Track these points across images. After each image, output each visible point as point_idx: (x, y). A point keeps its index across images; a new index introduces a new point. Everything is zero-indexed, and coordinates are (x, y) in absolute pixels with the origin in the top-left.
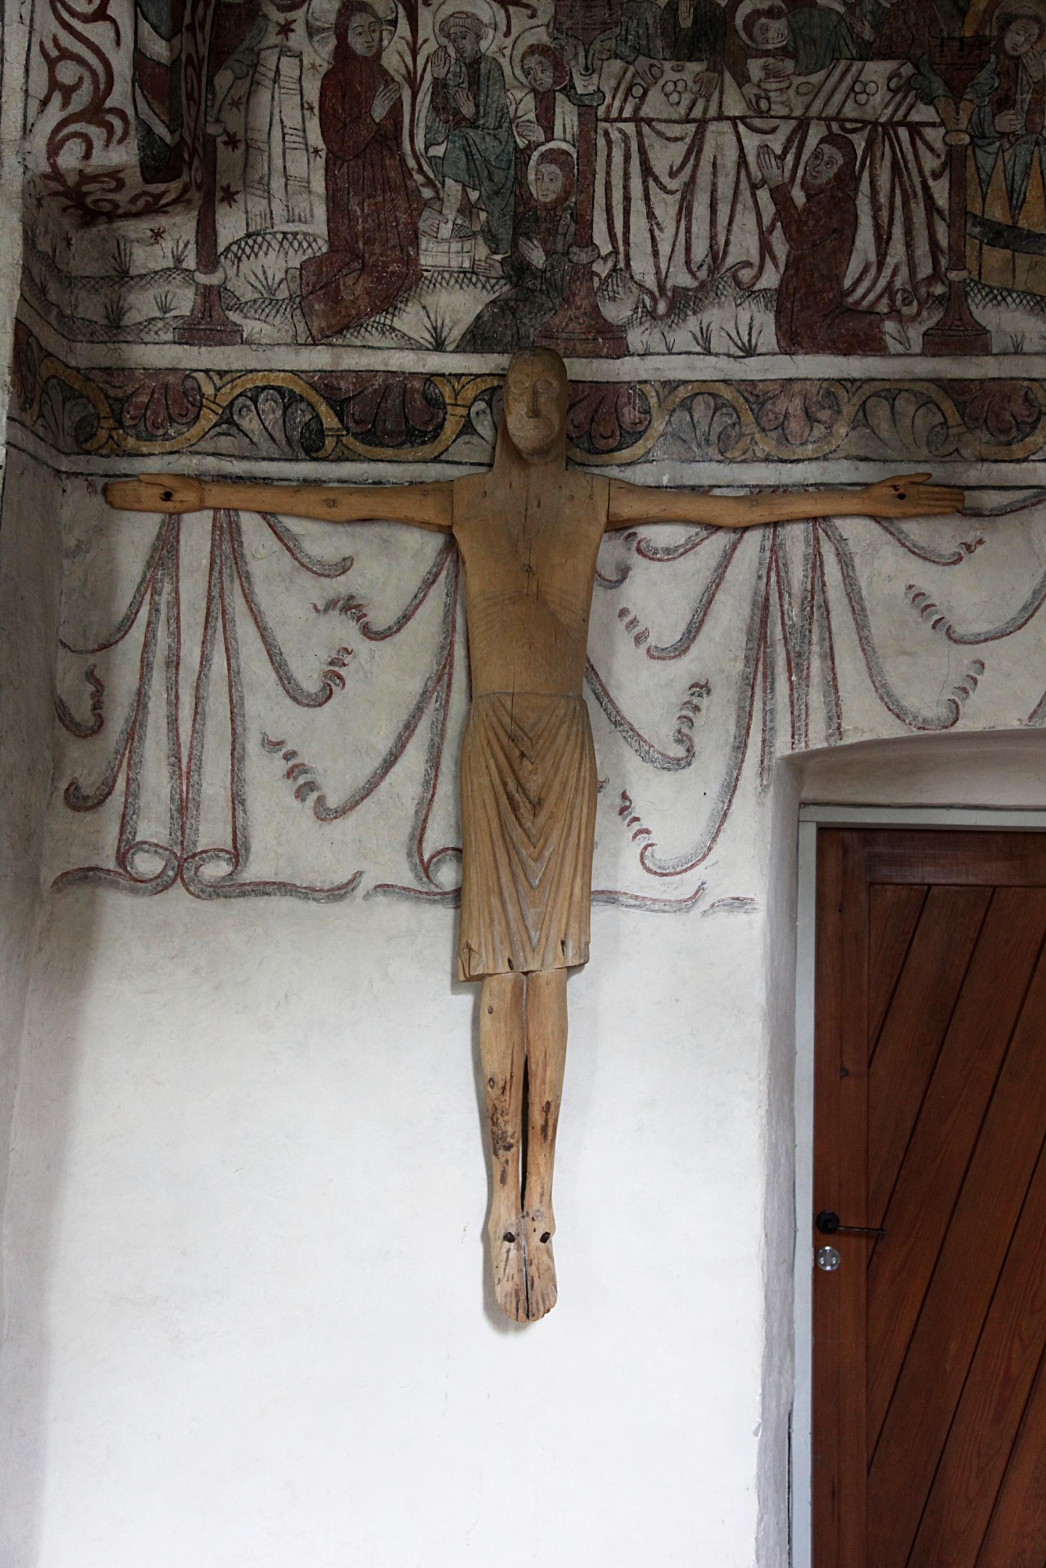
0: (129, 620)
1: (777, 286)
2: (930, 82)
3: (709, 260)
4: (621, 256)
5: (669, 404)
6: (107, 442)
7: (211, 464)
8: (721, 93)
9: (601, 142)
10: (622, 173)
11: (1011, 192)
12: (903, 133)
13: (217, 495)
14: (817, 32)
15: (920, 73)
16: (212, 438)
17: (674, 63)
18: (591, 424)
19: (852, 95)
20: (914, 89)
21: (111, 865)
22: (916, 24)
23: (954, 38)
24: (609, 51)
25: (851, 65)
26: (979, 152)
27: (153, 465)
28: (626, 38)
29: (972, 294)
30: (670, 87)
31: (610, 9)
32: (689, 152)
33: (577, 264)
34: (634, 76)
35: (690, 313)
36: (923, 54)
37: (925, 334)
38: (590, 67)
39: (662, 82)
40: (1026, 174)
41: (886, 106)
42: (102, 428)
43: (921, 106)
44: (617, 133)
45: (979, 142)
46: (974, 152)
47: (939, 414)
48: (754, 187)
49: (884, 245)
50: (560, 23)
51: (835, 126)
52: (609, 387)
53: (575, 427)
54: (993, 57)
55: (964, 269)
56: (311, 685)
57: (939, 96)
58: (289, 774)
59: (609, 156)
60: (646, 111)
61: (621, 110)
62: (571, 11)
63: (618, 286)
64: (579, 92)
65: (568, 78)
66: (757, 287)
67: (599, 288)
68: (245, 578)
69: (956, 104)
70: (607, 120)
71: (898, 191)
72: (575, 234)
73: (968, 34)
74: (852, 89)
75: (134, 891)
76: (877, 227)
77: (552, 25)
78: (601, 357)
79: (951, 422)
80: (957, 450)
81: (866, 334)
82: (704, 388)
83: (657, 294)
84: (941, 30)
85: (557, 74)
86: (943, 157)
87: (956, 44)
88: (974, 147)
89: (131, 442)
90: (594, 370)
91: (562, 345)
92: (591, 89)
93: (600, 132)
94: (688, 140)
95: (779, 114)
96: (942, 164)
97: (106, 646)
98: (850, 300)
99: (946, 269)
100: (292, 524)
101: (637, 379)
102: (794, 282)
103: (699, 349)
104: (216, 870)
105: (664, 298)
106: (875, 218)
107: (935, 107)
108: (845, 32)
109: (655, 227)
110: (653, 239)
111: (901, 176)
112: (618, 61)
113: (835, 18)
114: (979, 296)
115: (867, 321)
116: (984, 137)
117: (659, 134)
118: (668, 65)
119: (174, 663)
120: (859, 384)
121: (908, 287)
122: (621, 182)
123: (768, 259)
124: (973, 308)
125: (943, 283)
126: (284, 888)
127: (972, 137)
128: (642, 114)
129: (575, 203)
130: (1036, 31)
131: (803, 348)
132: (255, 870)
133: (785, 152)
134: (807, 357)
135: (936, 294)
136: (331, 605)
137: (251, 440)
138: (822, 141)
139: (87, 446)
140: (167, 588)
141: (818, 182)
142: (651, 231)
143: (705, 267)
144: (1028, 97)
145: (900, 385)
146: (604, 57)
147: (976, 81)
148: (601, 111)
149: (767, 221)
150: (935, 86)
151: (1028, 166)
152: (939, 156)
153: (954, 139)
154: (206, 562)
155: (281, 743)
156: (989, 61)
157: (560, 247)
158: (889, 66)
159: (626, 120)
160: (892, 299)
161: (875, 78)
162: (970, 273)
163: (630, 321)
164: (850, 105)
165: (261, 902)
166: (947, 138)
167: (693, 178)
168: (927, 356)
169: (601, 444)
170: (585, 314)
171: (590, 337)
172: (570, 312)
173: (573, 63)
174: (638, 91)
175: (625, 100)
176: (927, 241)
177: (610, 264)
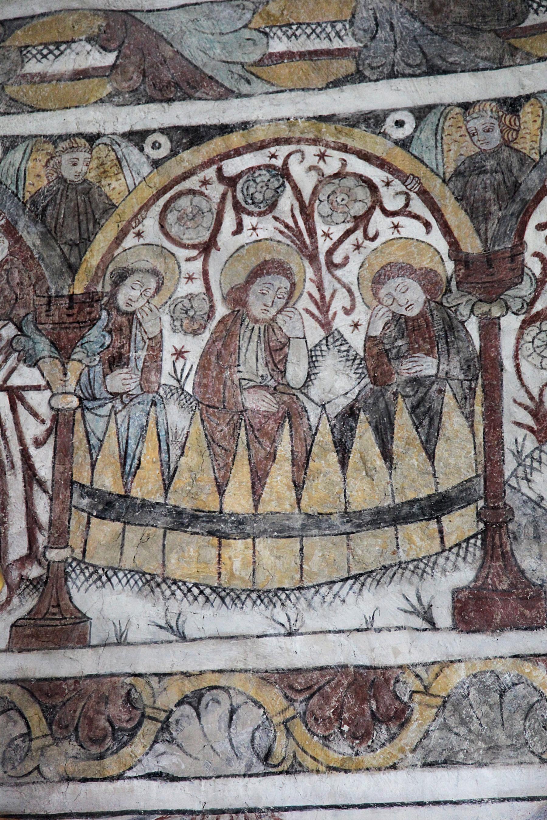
2: (35, 343)
11: (124, 458)
15: (23, 334)
20: (16, 351)
23: (63, 296)
26: (88, 415)
29: (73, 575)
36: (27, 314)
37: (13, 625)
40: (142, 438)
43: (23, 368)
45: (89, 405)
46: (83, 415)
47: (21, 723)
54: (104, 314)
55: (67, 546)
57: (44, 357)
69: (63, 365)
73: (77, 291)
79: (36, 732)
80: (38, 768)
84: (48, 288)
86: (48, 424)
87: (65, 302)
88: (83, 410)
96: (47, 430)
99: (45, 547)
107: (39, 369)
114: (82, 578)
116: (94, 399)
125: (40, 564)
127: (80, 399)
130: (153, 285)
135: (31, 577)
144: (143, 354)
147: (86, 339)
150: (39, 347)
151: (144, 428)
152: (43, 422)
153: (59, 403)
156: (100, 318)
162: (73, 551)
166: (53, 402)
168: (12, 651)
176: (24, 517)
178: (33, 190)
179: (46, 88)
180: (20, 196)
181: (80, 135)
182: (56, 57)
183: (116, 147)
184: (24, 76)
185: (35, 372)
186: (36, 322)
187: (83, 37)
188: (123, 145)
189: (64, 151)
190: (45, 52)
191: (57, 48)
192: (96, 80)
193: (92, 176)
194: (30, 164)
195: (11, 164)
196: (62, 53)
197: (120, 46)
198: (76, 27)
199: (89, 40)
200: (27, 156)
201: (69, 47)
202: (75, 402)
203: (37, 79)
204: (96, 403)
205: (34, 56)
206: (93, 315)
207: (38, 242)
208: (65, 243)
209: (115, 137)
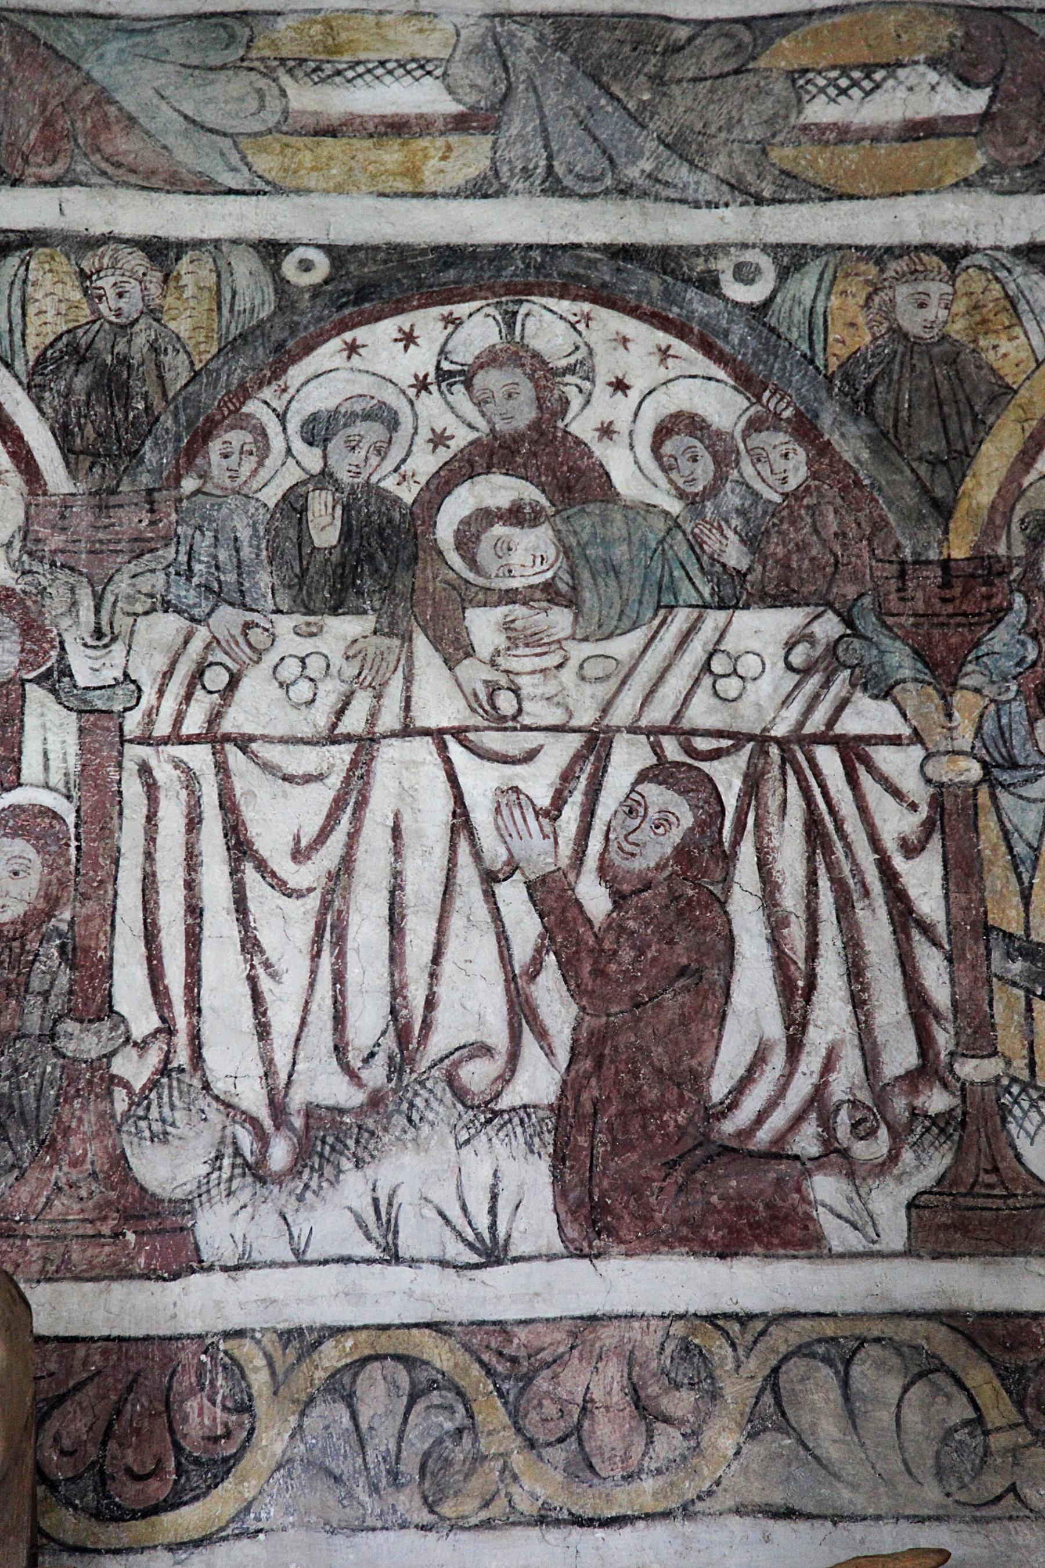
1: (553, 1099)
2: (882, 652)
3: (390, 1042)
4: (181, 1039)
5: (299, 1385)
8: (408, 680)
9: (133, 789)
10: (181, 854)
12: (828, 759)
14: (620, 553)
15: (857, 634)
17: (298, 619)
18: (104, 1443)
19: (707, 681)
20: (846, 667)
22: (841, 535)
23: (928, 562)
24: (151, 596)
25: (700, 619)
26: (1005, 799)
28: (190, 569)
29: (1017, 1111)
30: (291, 669)
31: (152, 511)
32: (338, 804)
33: (75, 1060)
34: (208, 647)
35: (347, 1165)
36: (861, 595)
37: (911, 1205)
38: (106, 629)
39: (271, 658)
41: (786, 702)
43: (862, 701)
44: (169, 767)
45: (1005, 777)
46: (994, 797)
47: (962, 1399)
48: (490, 878)
49: (799, 1002)
50: (38, 541)
51: (672, 749)
52: (154, 1349)
53: (63, 1453)
54: (1019, 600)
55: (994, 1053)
57: (904, 681)
59: (151, 818)
60: (233, 722)
61: (179, 720)
62: (63, 517)
63: (172, 1107)
64: (82, 681)
65: (54, 653)
66: (504, 1103)
67: (127, 1115)
69: (944, 697)
70: (145, 740)
71: (824, 883)
72: (71, 992)
73: (956, 554)
74: (707, 667)
76: (781, 961)
77: (17, 544)
78: (131, 1277)
79: (993, 1418)
80: (1013, 1489)
81: (768, 1206)
82: (385, 1344)
83: (268, 1123)
84: (898, 546)
85: (28, 645)
86: (924, 811)
88: (992, 787)
90: (115, 1310)
91: (36, 1253)
92: (108, 676)
93: (130, 766)
94: (335, 781)
95: (544, 723)
96: (923, 824)
98: (729, 1126)
99: (952, 1054)
101: (220, 1328)
102: (593, 1091)
103: (370, 1250)
105: (285, 1131)
106: (775, 942)
107: (895, 702)
108: (683, 551)
109: (260, 971)
110: (256, 997)
111: (828, 850)
112: (172, 617)
113: (661, 525)
115: (772, 1175)
116: (1014, 766)
117: (267, 767)
118: (284, 624)
120: (759, 1325)
121: (864, 1096)
122: (180, 876)
123: (528, 1037)
124: (1022, 1143)
125: (945, 1086)
127: (985, 766)
128: (228, 725)
129: (72, 923)
131: (621, 1241)
133: (559, 800)
134: (634, 1264)
135: (932, 1112)
138: (643, 777)
141: (637, 865)
142: (252, 981)
143: (381, 1059)
145: (861, 1328)
146: (139, 608)
147: (984, 649)
148: (132, 724)
149: (522, 952)
152: (913, 807)
153: (943, 770)
156: (1010, 608)
157: (33, 1023)
158: (790, 619)
159: (189, 741)
160: (827, 1123)
161: (756, 646)
162: (1008, 1063)
163: (203, 1191)
164: (702, 698)
166: (929, 770)
167: (347, 862)
168: (919, 1257)
169: (127, 1493)
170: (94, 1175)
171: (106, 1230)
172: (56, 1172)
173: (65, 622)
174: (217, 678)
175: (188, 697)
176: (901, 995)
177: (154, 1057)
178: (844, 352)
179: (851, 155)
180: (820, 362)
181: (929, 248)
182: (867, 94)
183: (1002, 274)
184: (805, 128)
185: (889, 708)
186: (881, 612)
187: (922, 57)
188: (1018, 270)
189: (900, 277)
190: (844, 83)
191: (868, 76)
192: (952, 142)
193: (957, 329)
194: (835, 301)
195: (797, 301)
196: (878, 86)
197: (997, 77)
198: (905, 37)
199: (933, 63)
200: (825, 285)
201: (892, 75)
202: (975, 771)
203: (832, 136)
204: (1019, 775)
205: (822, 90)
206: (996, 601)
207: (865, 455)
208: (920, 459)
209: (999, 255)
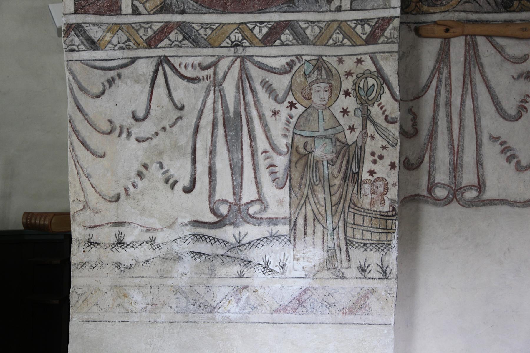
0: (427, 86)
6: (415, 8)
7: (463, 15)
13: (470, 29)
16: (462, 4)
21: (425, 193)
27: (437, 17)
42: (413, 2)
56: (512, 112)
58: (503, 151)
68: (481, 66)
75: (435, 205)
89: (425, 8)
97: (417, 98)
100: (501, 41)
104: (470, 194)
119: (449, 104)
126: (503, 202)
132: (490, 194)
136: (520, 76)
137: (479, 4)
139: (407, 10)
140: (445, 71)
154: (462, 59)
155: (498, 138)
165: (493, 208)
